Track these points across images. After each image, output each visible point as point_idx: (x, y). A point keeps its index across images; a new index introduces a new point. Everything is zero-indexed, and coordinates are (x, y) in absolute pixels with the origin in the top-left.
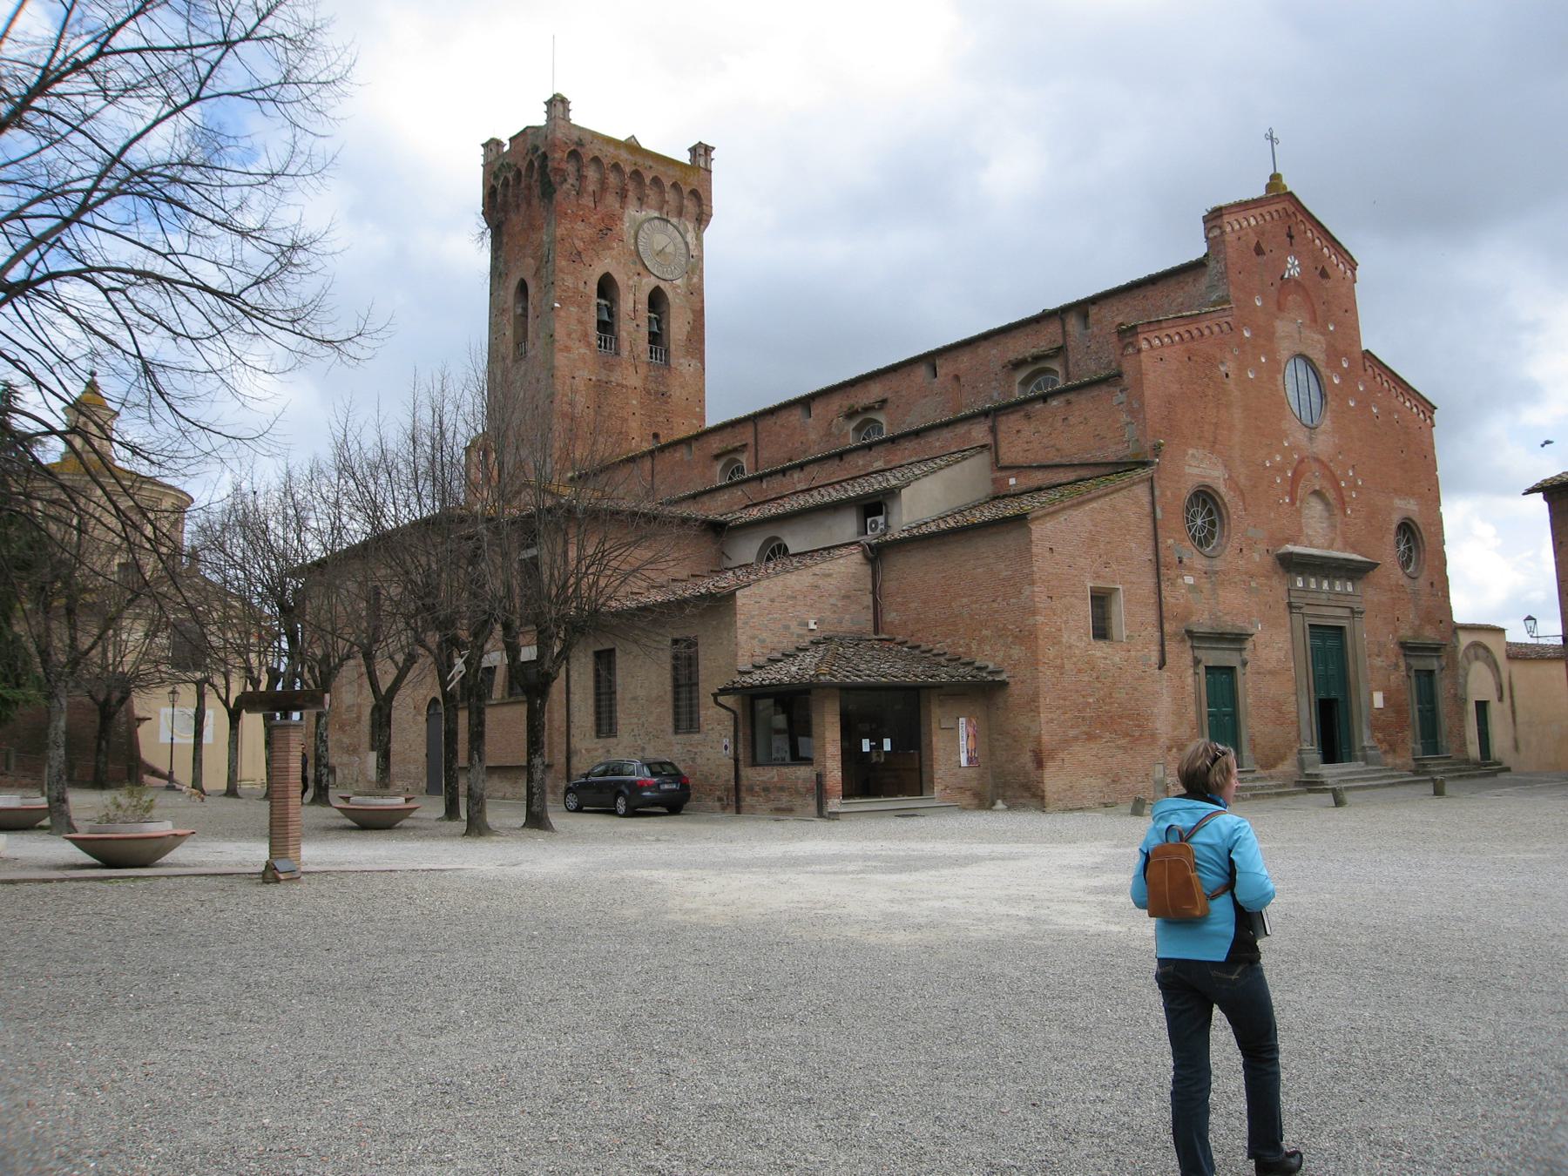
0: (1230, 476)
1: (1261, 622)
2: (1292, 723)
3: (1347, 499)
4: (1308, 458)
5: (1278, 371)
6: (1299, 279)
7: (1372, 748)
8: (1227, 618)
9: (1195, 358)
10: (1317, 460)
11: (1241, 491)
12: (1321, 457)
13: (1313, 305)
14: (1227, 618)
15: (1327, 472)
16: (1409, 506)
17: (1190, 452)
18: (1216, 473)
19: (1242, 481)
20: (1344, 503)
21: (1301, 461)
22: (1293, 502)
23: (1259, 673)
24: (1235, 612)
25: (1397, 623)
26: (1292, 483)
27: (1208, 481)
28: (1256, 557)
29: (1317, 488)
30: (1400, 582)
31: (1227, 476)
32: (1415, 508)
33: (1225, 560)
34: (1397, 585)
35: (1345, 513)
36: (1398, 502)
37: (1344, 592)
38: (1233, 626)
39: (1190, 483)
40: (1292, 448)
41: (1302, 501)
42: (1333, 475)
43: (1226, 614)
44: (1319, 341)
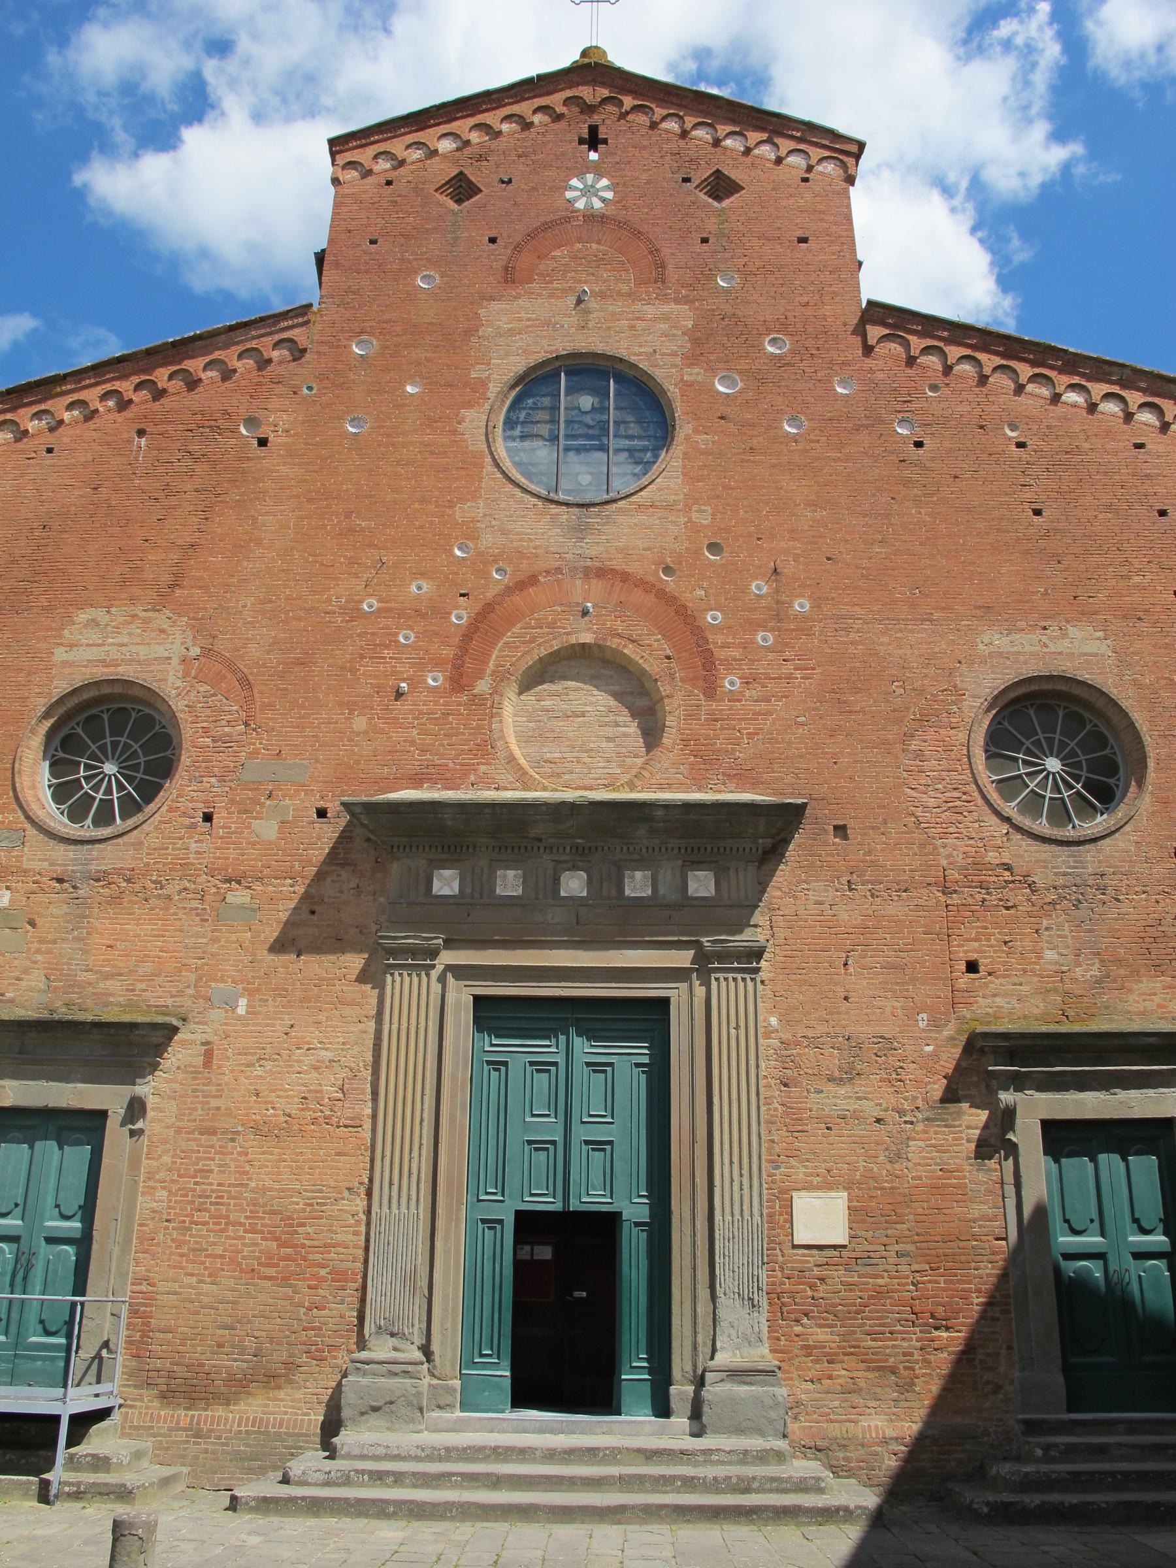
0: (207, 652)
1: (250, 992)
2: (339, 1276)
3: (720, 654)
4: (559, 570)
5: (469, 405)
6: (611, 211)
7: (737, 1374)
8: (113, 985)
9: (161, 428)
10: (602, 573)
11: (246, 683)
12: (618, 564)
13: (654, 251)
14: (113, 985)
15: (638, 596)
16: (1063, 645)
17: (82, 617)
18: (160, 651)
19: (254, 651)
20: (709, 662)
21: (521, 585)
22: (459, 681)
23: (211, 1132)
24: (148, 967)
25: (964, 980)
26: (464, 647)
27: (126, 672)
28: (267, 829)
29: (587, 638)
30: (992, 857)
31: (195, 651)
32: (1103, 648)
33: (138, 845)
34: (979, 865)
35: (711, 690)
36: (994, 640)
37: (674, 897)
38: (131, 1006)
39: (61, 687)
40: (482, 562)
41: (500, 677)
42: (662, 594)
43: (108, 976)
44: (665, 318)
